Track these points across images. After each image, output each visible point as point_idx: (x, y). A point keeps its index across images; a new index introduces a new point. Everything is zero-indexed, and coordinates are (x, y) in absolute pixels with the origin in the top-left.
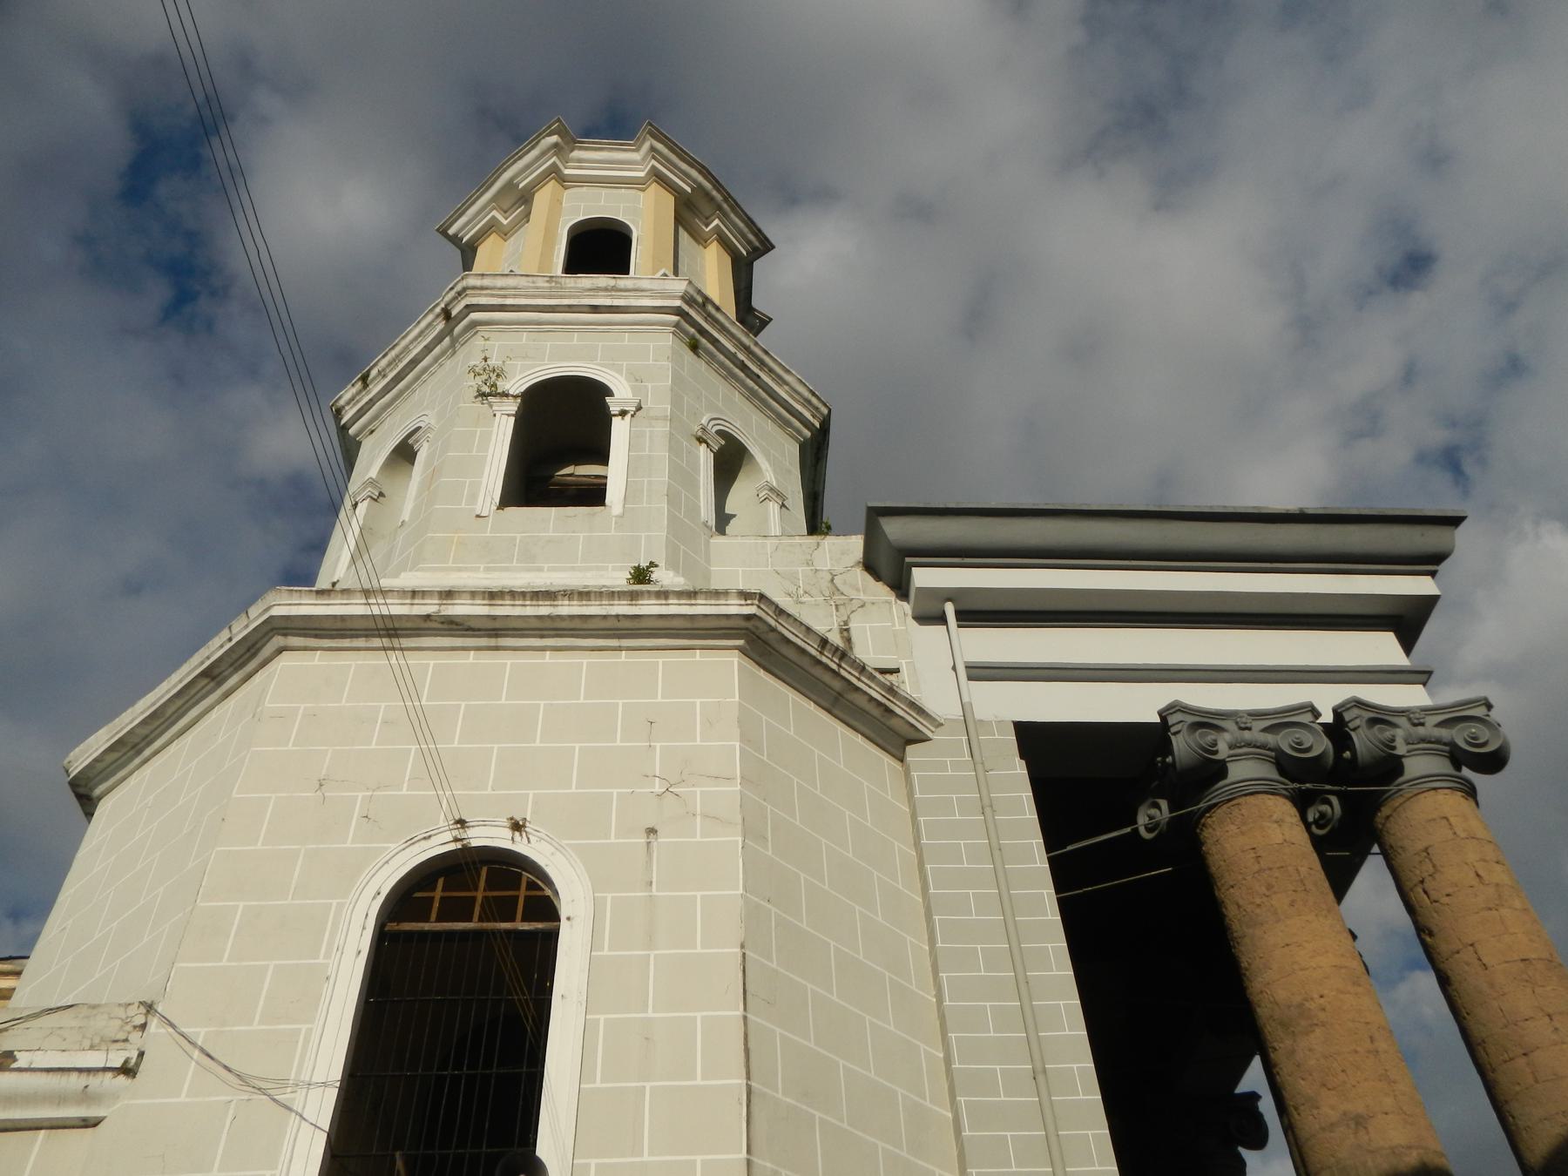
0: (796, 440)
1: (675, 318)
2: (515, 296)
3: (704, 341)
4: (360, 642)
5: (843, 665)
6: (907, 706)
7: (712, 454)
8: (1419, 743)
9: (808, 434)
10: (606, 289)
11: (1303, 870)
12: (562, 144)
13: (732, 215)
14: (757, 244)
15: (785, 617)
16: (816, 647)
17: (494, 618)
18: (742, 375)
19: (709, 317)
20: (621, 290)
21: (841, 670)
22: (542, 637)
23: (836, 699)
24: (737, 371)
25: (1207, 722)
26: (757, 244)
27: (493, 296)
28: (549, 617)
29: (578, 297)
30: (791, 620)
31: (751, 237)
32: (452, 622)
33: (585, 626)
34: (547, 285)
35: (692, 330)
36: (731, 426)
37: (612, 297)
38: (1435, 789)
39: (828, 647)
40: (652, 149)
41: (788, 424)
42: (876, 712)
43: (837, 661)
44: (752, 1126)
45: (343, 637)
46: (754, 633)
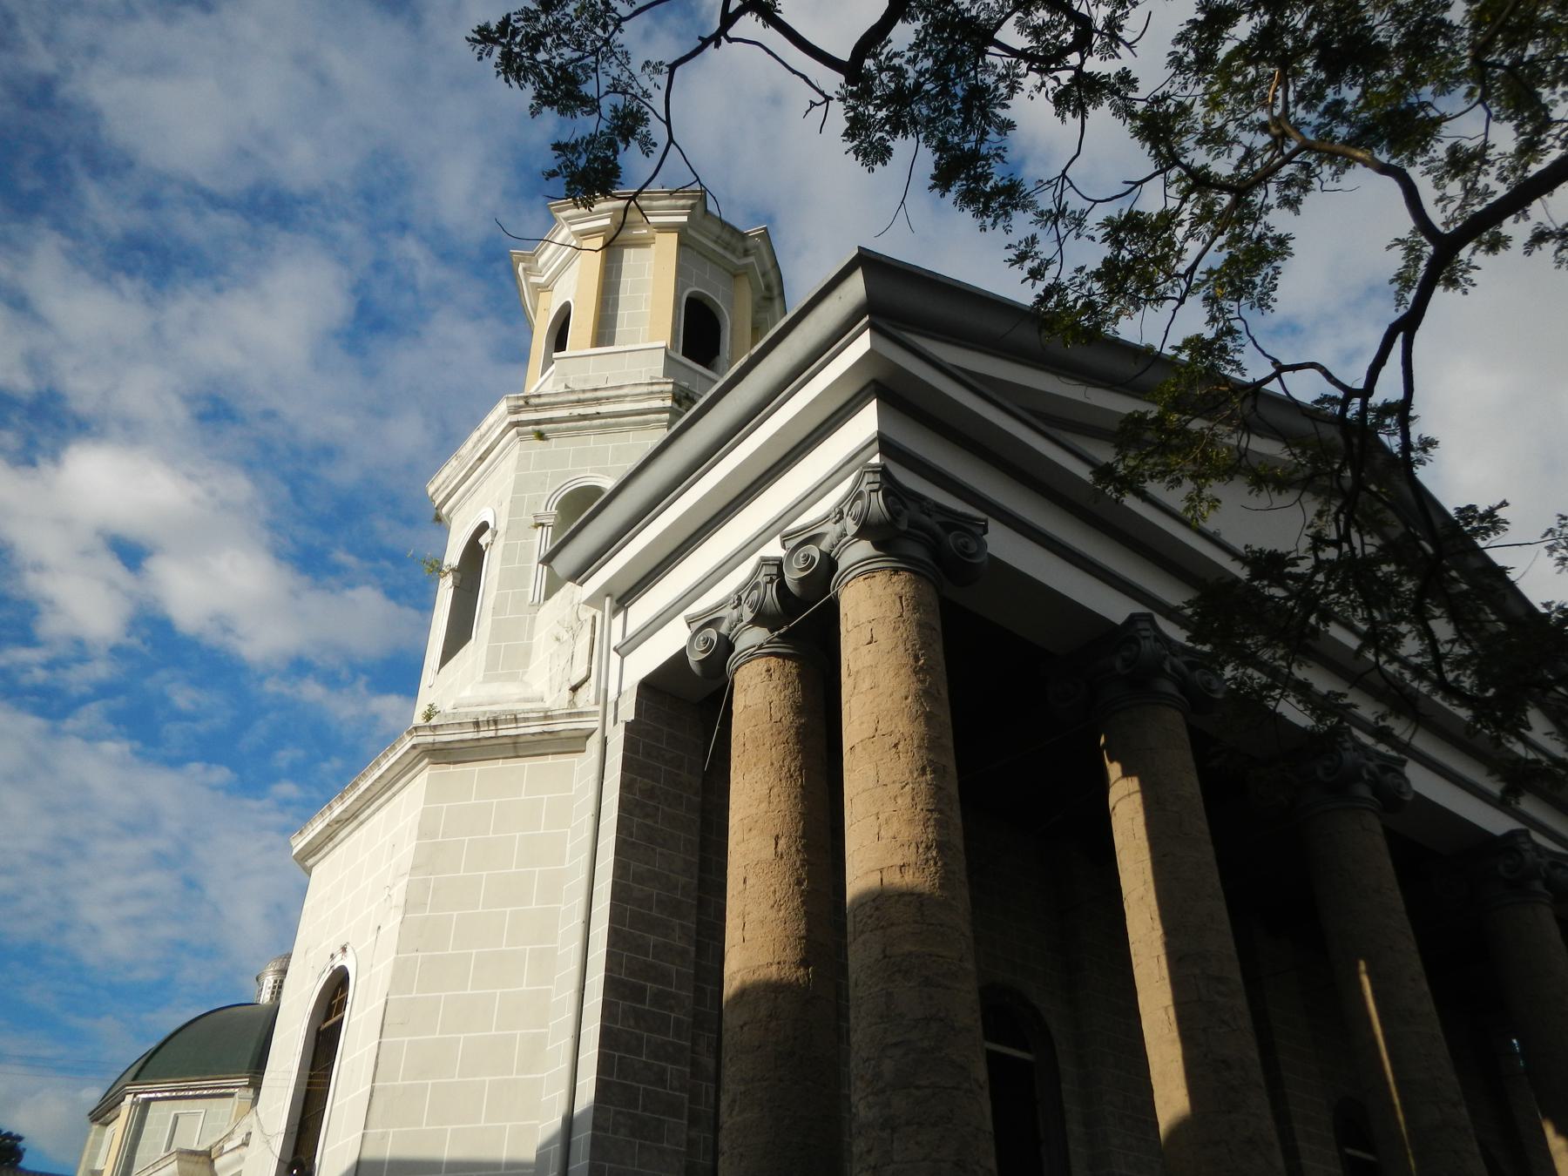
0: (662, 427)
1: (514, 431)
2: (451, 482)
3: (543, 427)
4: (326, 850)
5: (500, 727)
6: (567, 718)
7: (550, 528)
8: (839, 541)
9: (666, 416)
10: (479, 441)
11: (747, 731)
12: (528, 265)
13: (655, 203)
14: (690, 202)
15: (439, 728)
16: (472, 730)
17: (344, 811)
18: (586, 423)
19: (538, 408)
20: (485, 435)
21: (500, 731)
22: (369, 807)
23: (515, 747)
24: (581, 423)
25: (711, 621)
26: (690, 202)
27: (443, 491)
28: (357, 798)
29: (473, 457)
30: (445, 727)
31: (681, 202)
32: (338, 822)
33: (373, 794)
34: (457, 462)
35: (530, 428)
36: (562, 490)
37: (484, 443)
38: (847, 584)
39: (481, 723)
40: (566, 219)
41: (646, 423)
42: (546, 737)
43: (493, 728)
44: (372, 1110)
45: (320, 850)
46: (429, 751)
